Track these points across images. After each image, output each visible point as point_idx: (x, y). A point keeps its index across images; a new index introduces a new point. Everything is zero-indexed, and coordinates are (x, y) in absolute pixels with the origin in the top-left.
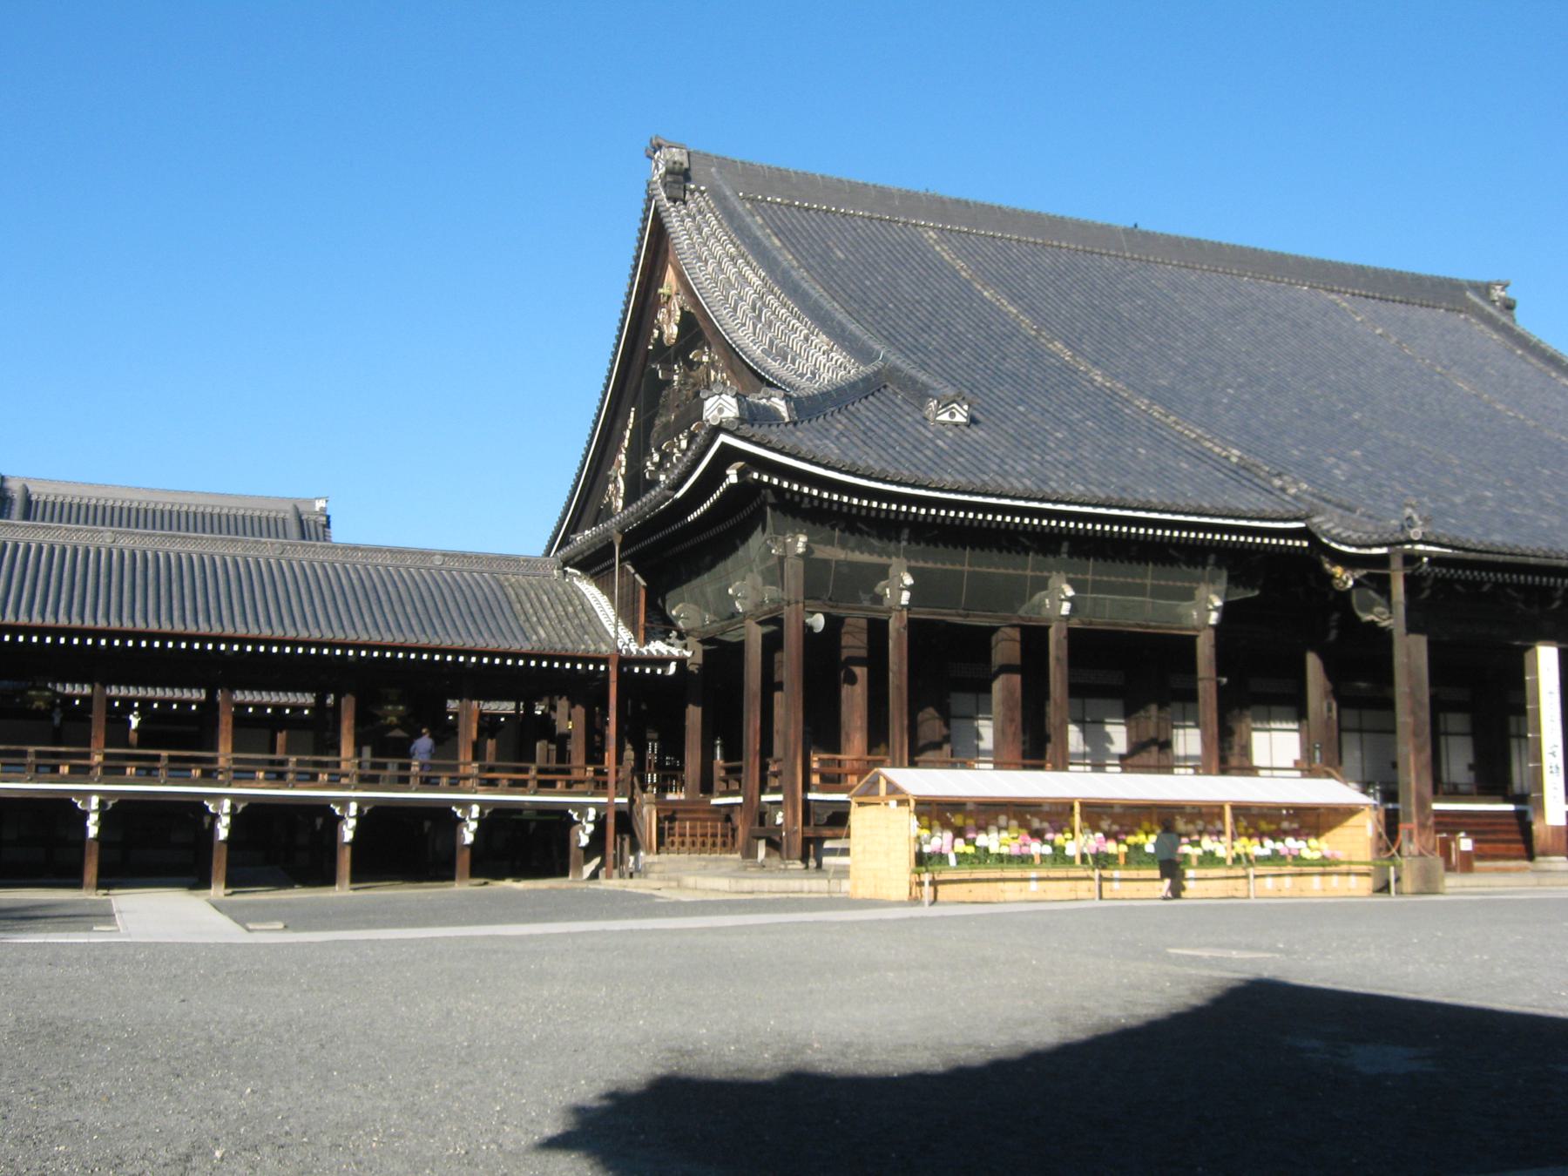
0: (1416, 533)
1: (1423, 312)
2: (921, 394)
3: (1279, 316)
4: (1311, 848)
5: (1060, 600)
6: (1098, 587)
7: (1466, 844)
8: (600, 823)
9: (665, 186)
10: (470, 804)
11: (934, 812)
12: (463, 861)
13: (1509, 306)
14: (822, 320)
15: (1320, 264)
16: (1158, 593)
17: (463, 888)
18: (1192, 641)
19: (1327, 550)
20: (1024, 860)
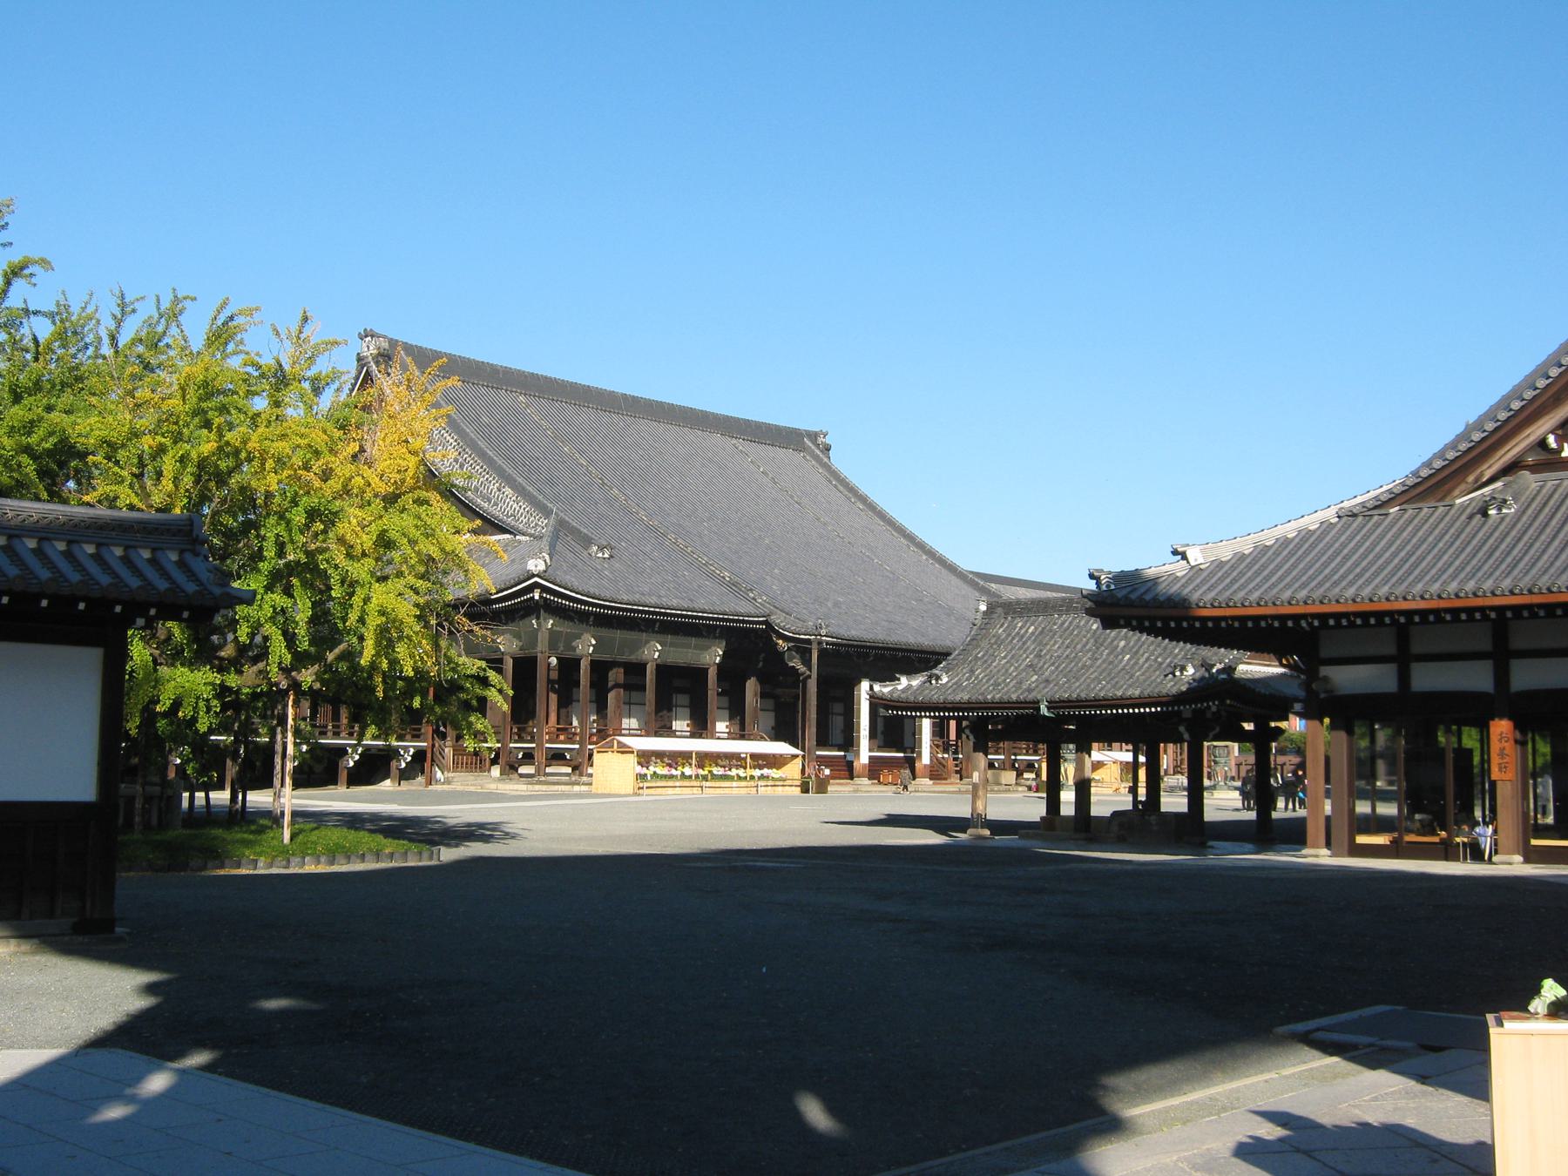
0: (823, 632)
1: (781, 452)
2: (587, 541)
3: (711, 461)
4: (774, 773)
5: (654, 651)
6: (672, 645)
7: (827, 772)
8: (420, 756)
9: (377, 363)
10: (354, 747)
11: (645, 757)
12: (343, 776)
13: (828, 449)
14: (509, 481)
15: (727, 419)
16: (696, 647)
17: (341, 789)
18: (706, 671)
19: (777, 632)
20: (671, 777)
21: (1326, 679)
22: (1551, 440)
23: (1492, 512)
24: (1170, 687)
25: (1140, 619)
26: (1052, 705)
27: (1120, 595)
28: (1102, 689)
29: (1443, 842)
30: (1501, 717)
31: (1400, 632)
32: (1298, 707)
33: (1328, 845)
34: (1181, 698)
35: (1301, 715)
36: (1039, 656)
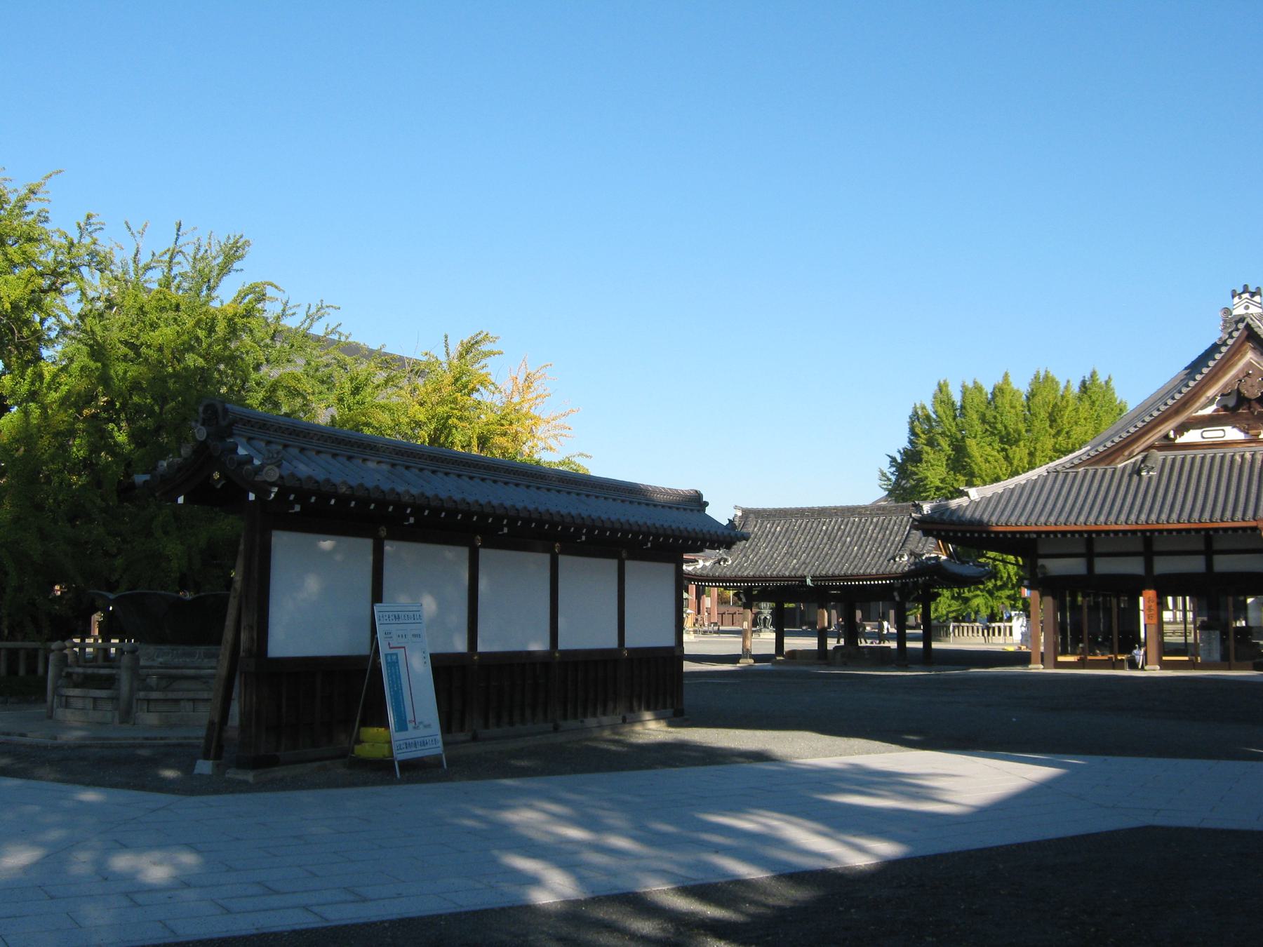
21: (1043, 566)
22: (1172, 435)
23: (1144, 474)
24: (893, 568)
25: (939, 531)
26: (814, 579)
27: (936, 516)
28: (847, 568)
29: (1110, 659)
30: (1150, 588)
31: (1089, 543)
32: (1026, 582)
33: (1042, 662)
34: (904, 575)
35: (1029, 587)
36: (790, 546)
